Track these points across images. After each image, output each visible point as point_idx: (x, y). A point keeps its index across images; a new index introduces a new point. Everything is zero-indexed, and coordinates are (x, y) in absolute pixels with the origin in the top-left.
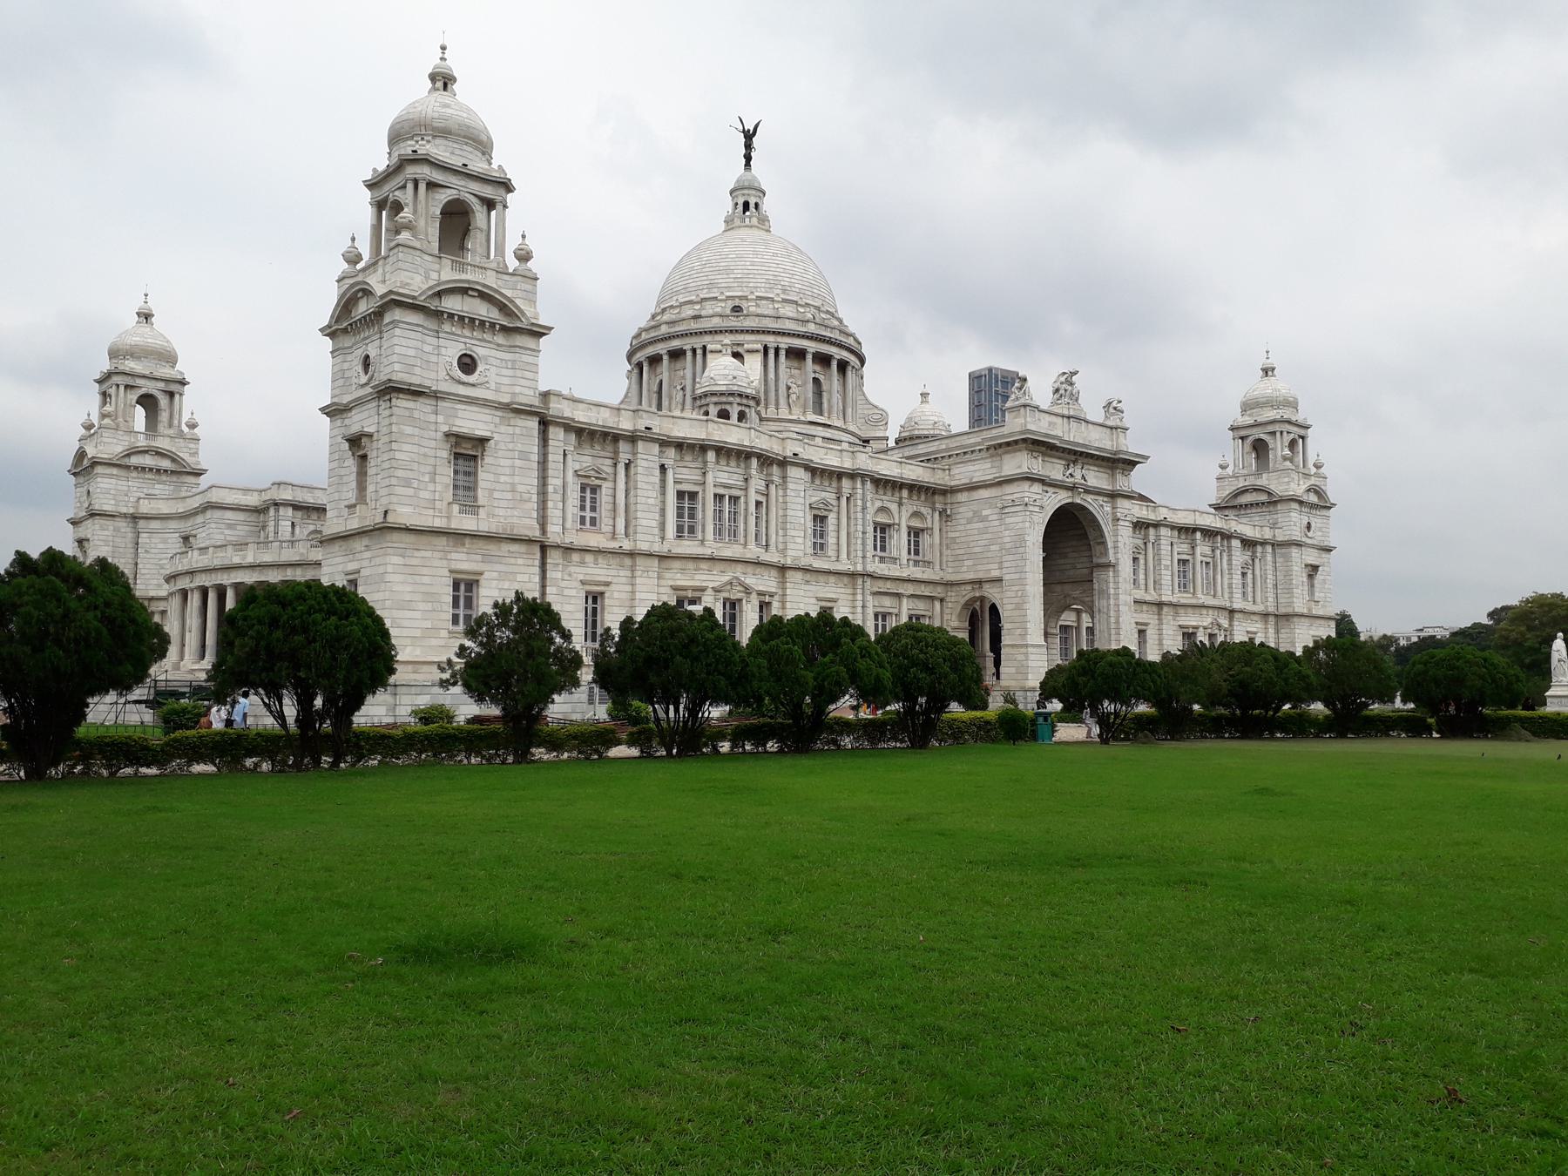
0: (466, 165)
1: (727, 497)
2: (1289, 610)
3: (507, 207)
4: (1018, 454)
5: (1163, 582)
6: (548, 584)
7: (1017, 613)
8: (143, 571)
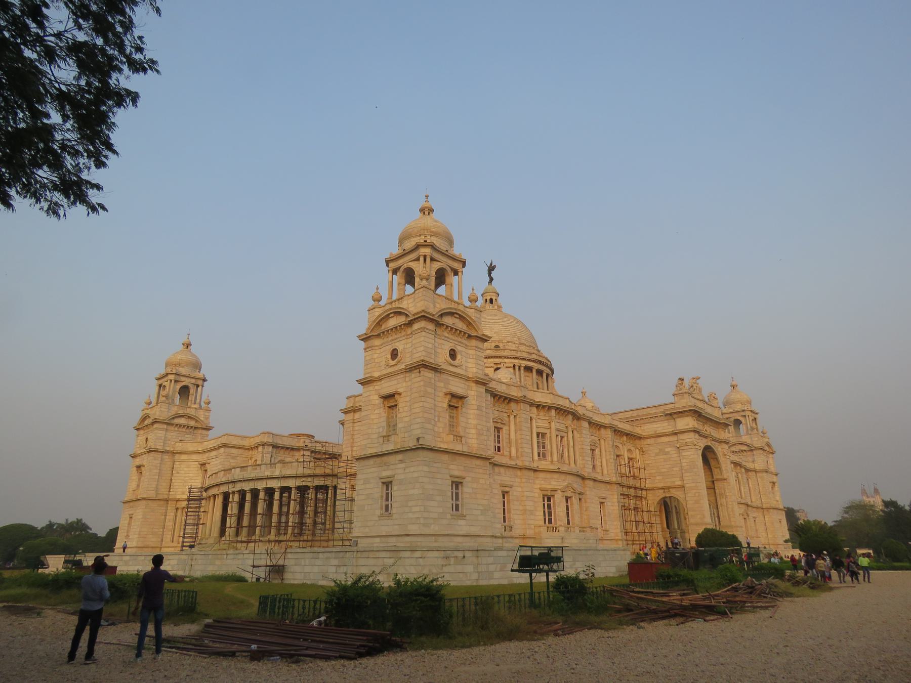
4: (686, 418)
8: (175, 484)
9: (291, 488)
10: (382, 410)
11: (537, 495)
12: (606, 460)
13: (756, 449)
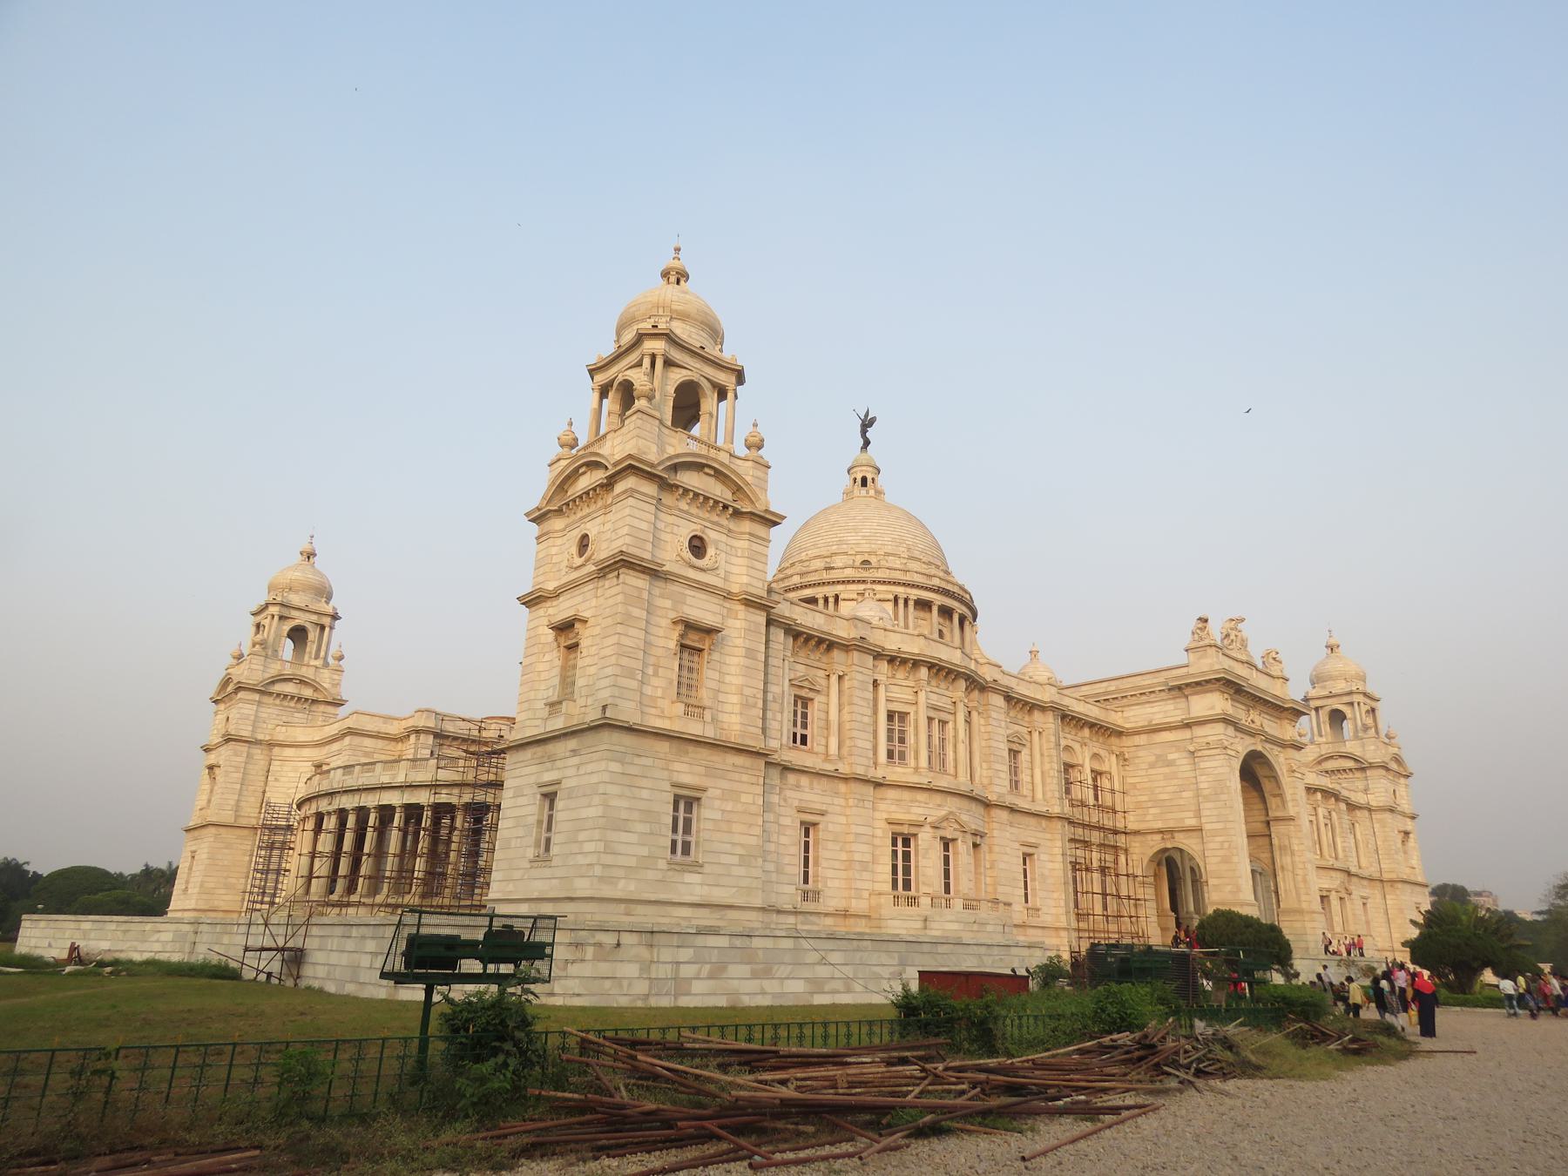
4: (1209, 695)
9: (395, 808)
10: (555, 653)
11: (879, 833)
12: (1042, 773)
13: (1372, 766)
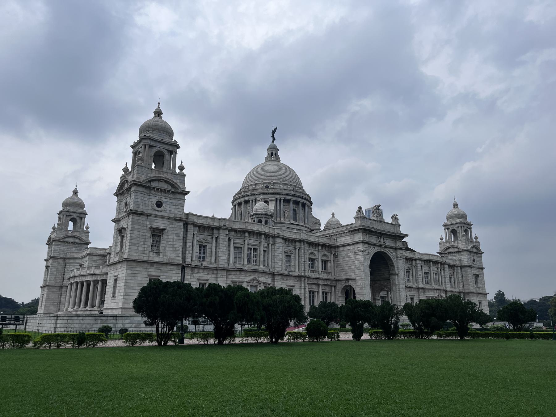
0: (163, 140)
1: (253, 249)
2: (468, 291)
3: (177, 153)
4: (359, 234)
5: (419, 280)
6: (185, 280)
7: (361, 291)
